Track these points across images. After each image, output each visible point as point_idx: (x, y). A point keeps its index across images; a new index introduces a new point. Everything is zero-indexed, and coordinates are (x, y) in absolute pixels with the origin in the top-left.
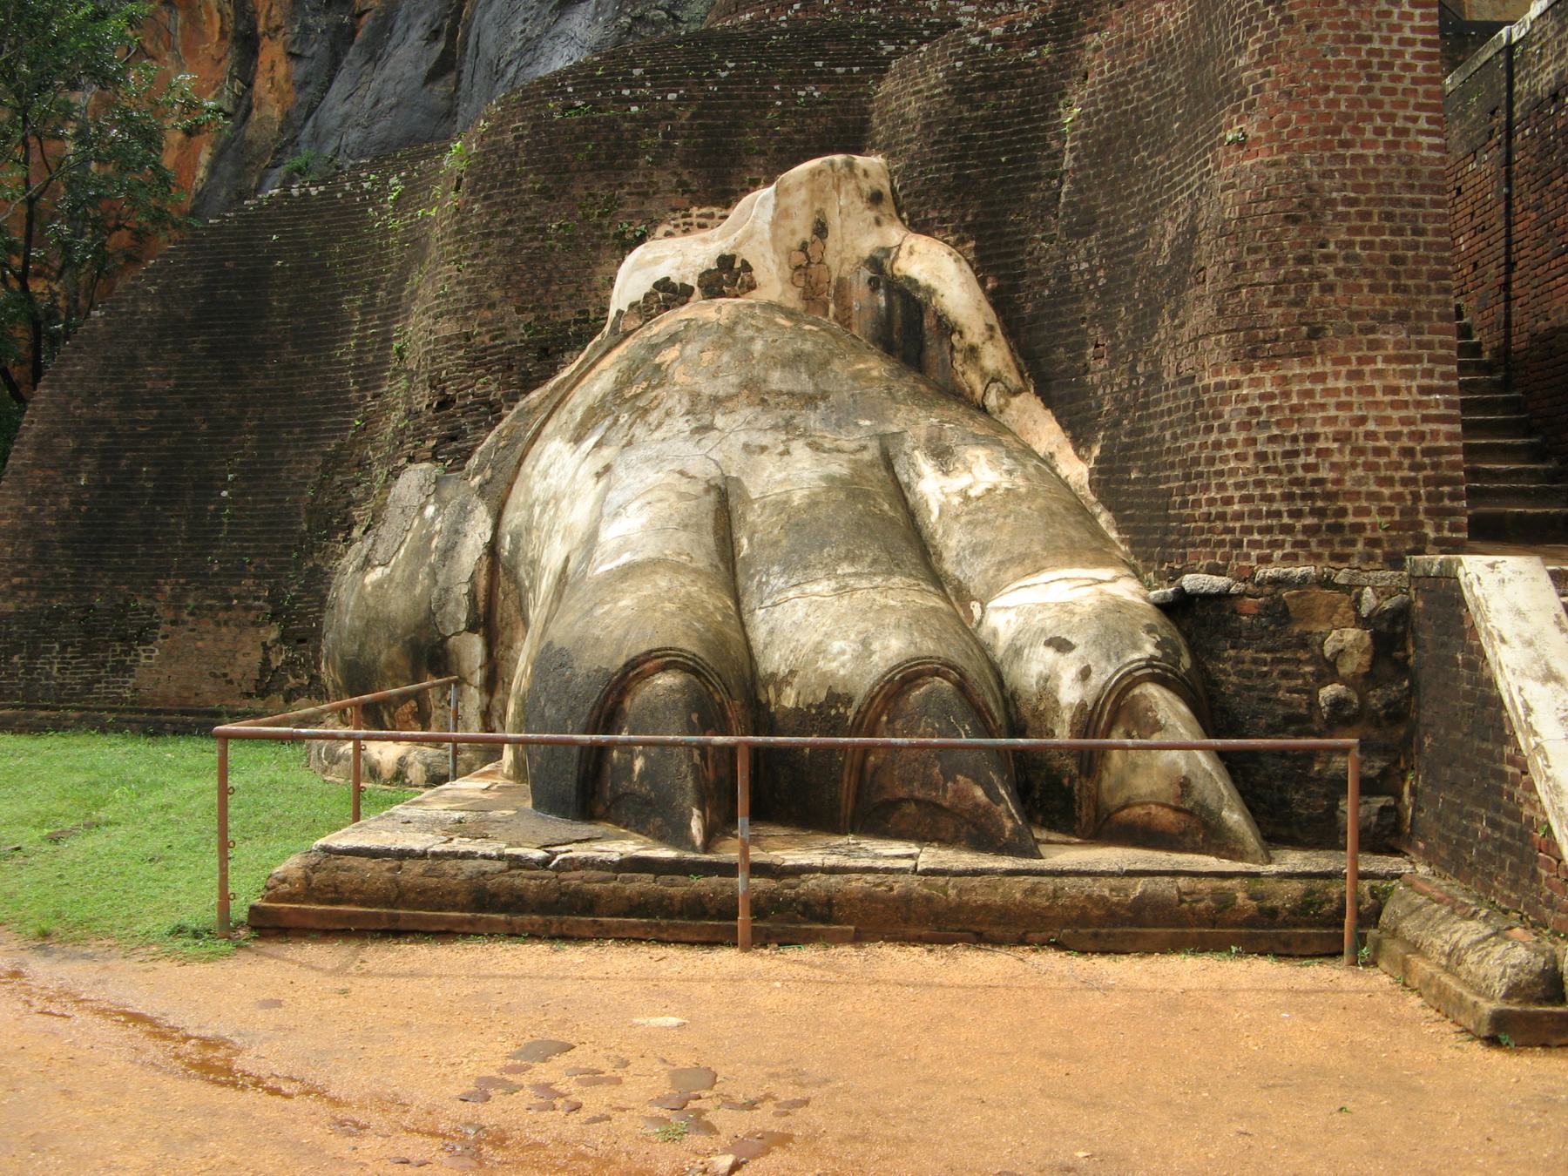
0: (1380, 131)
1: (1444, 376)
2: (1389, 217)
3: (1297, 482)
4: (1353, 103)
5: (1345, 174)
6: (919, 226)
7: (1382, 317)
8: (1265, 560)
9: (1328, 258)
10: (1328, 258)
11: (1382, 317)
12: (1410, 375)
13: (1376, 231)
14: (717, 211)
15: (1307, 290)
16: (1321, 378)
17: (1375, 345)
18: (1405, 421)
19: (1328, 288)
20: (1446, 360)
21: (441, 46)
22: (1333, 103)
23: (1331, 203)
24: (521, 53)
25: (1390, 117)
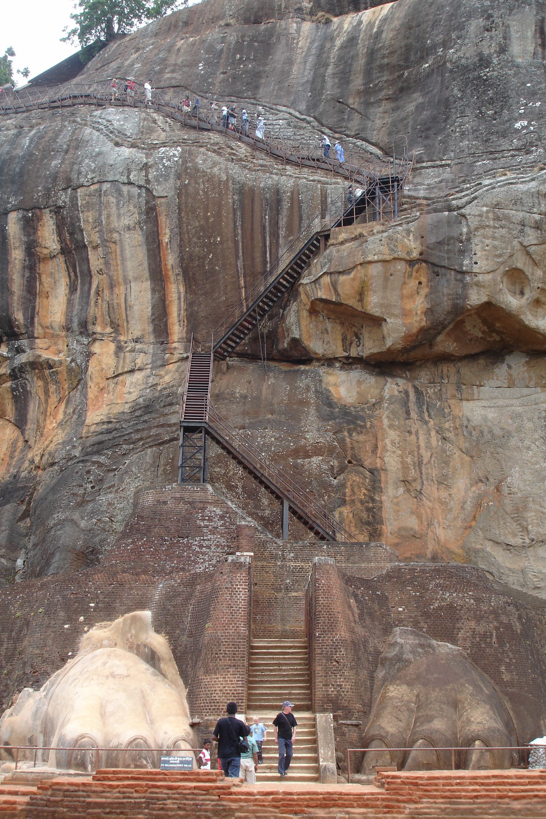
0: (233, 627)
1: (242, 678)
2: (233, 645)
3: (212, 700)
4: (229, 621)
5: (226, 636)
6: (157, 631)
7: (230, 666)
8: (206, 715)
9: (221, 654)
10: (221, 654)
11: (230, 666)
12: (235, 678)
13: (231, 648)
14: (109, 623)
15: (216, 660)
16: (218, 678)
17: (228, 672)
18: (233, 687)
19: (220, 660)
20: (243, 675)
21: (24, 507)
22: (225, 621)
23: (222, 642)
24: (55, 525)
25: (236, 624)
